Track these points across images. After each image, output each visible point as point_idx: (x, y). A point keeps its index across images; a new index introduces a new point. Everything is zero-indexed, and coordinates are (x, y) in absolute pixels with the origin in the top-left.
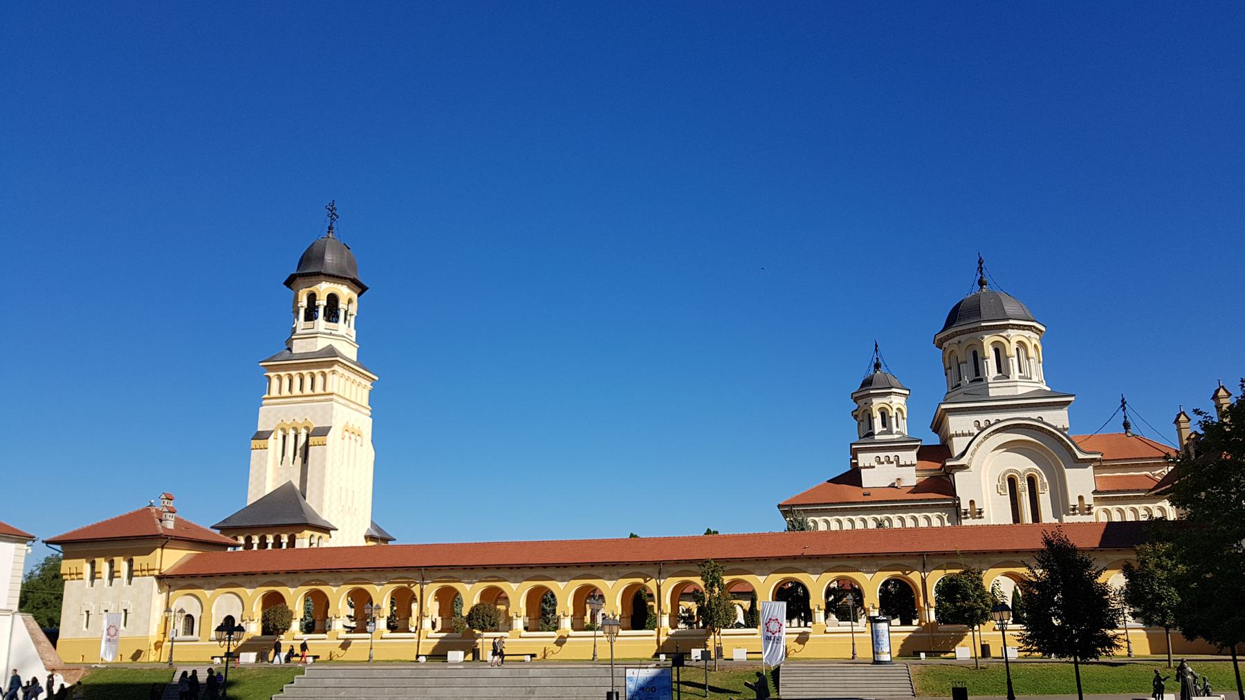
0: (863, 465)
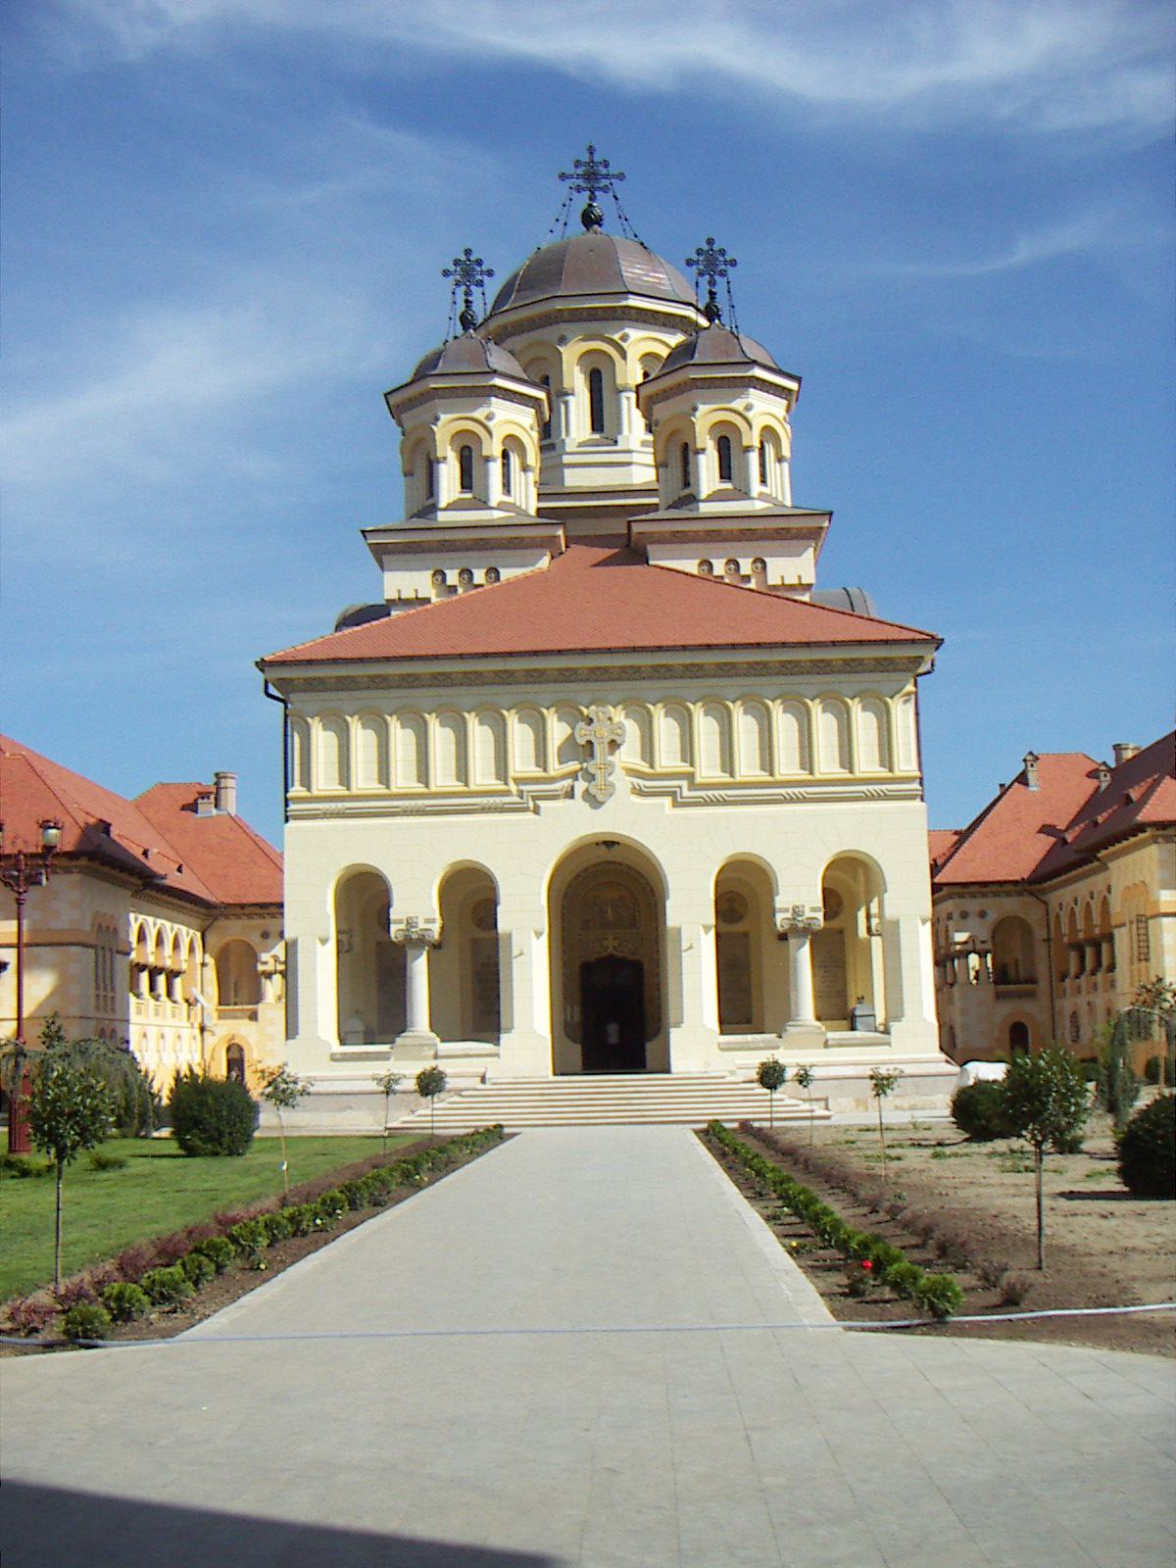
0: (395, 596)
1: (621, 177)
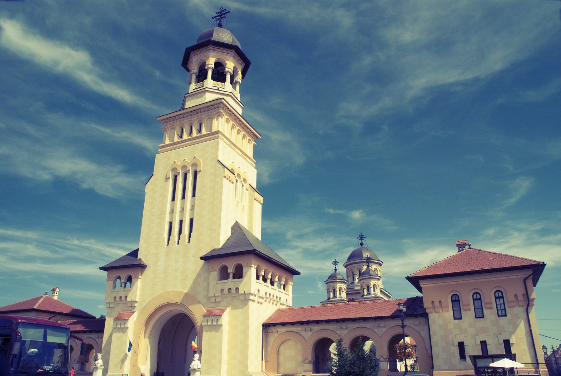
1: (366, 237)
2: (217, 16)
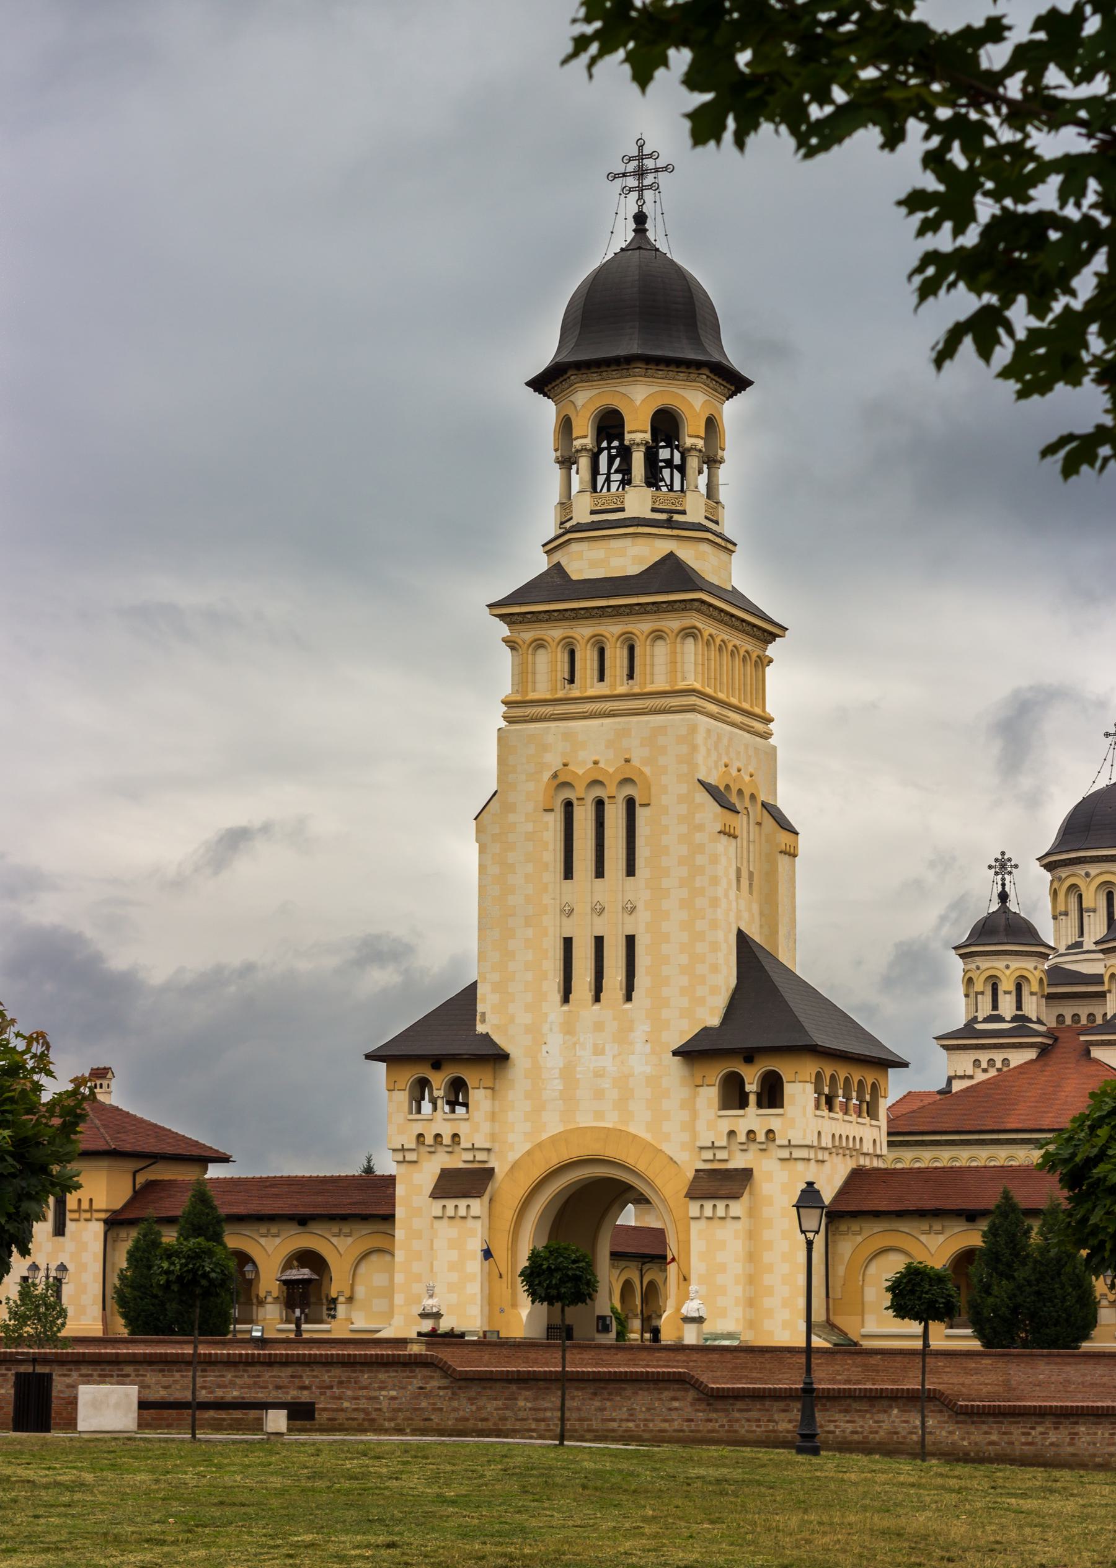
2: (624, 175)
